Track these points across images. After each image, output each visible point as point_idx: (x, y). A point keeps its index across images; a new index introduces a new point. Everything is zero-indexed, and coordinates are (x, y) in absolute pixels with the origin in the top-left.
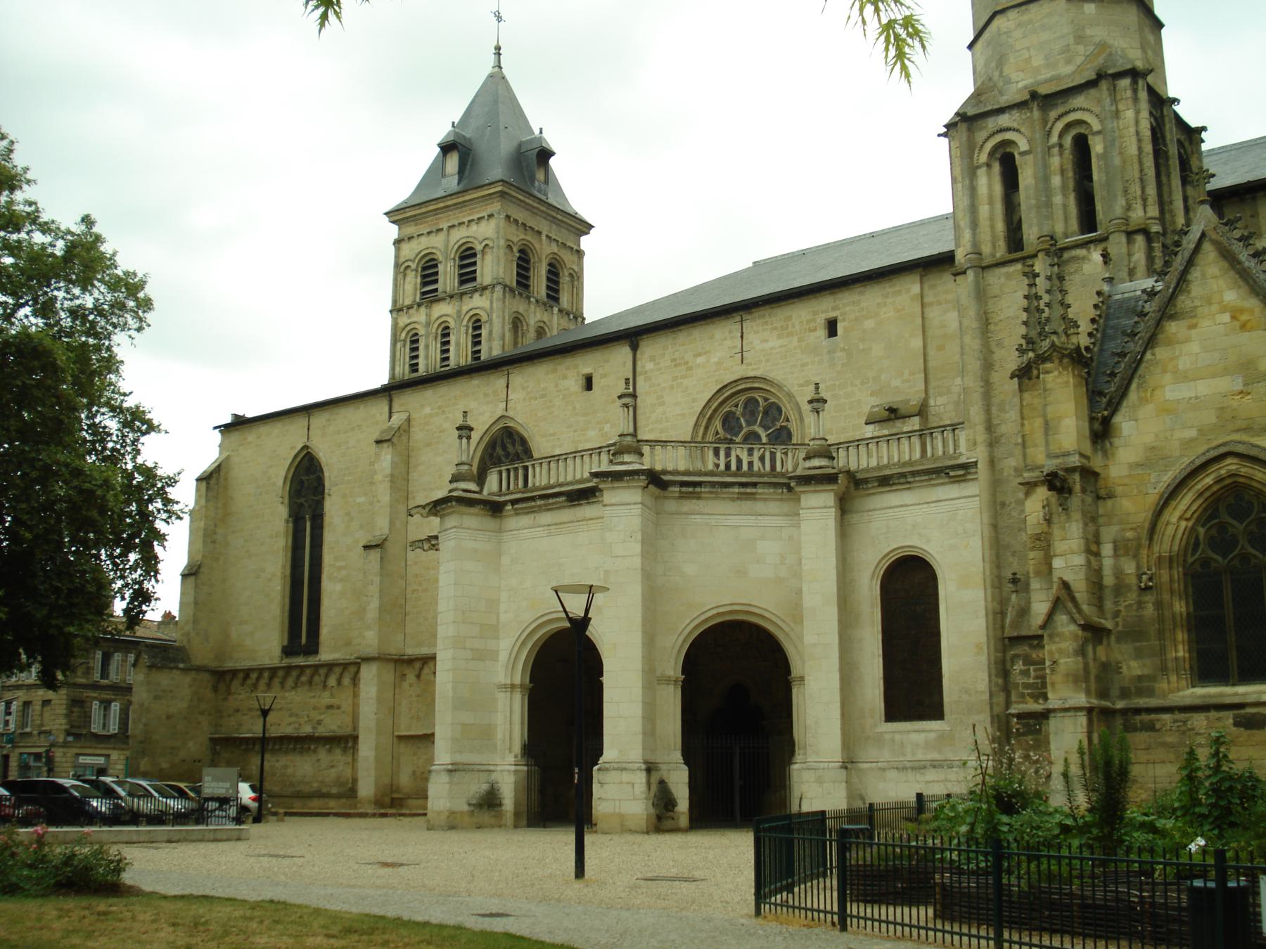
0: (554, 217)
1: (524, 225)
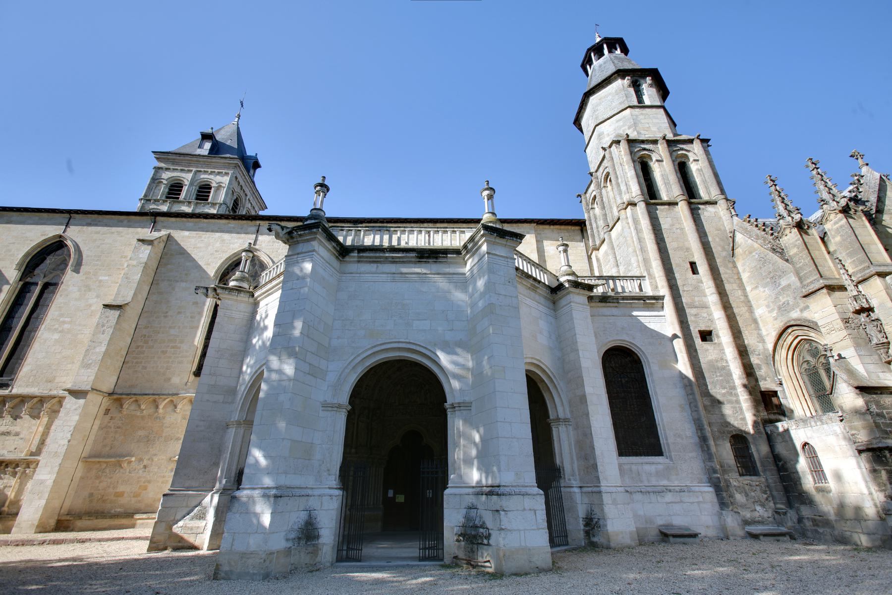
0: (254, 193)
1: (241, 186)
